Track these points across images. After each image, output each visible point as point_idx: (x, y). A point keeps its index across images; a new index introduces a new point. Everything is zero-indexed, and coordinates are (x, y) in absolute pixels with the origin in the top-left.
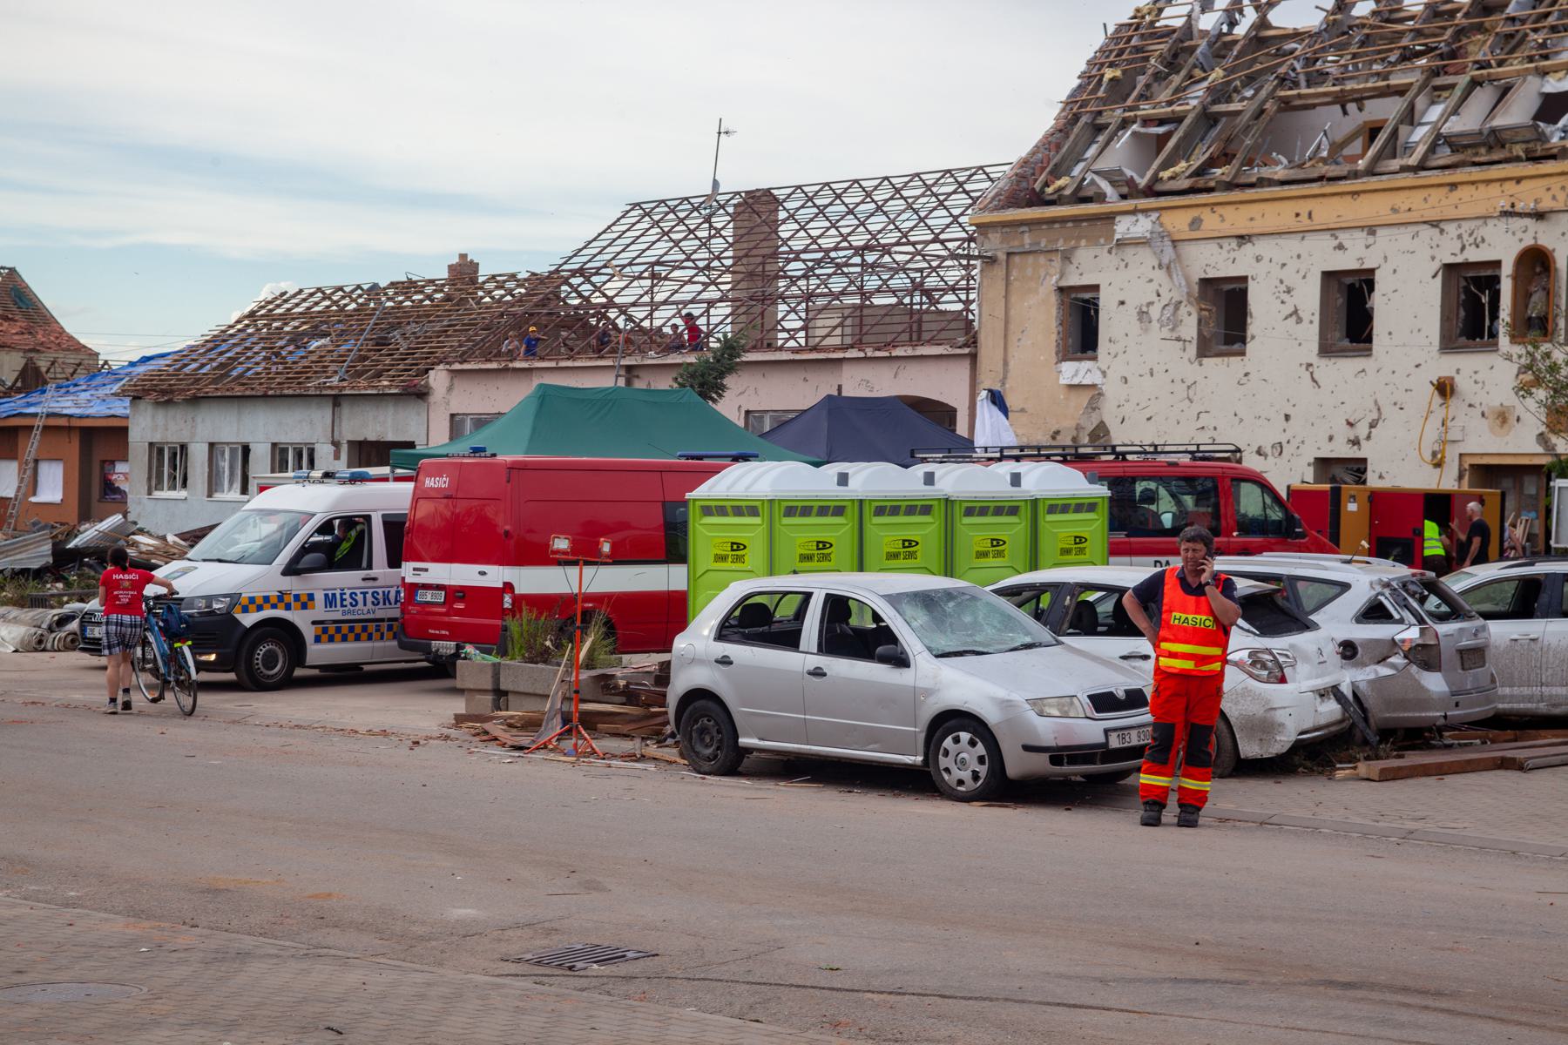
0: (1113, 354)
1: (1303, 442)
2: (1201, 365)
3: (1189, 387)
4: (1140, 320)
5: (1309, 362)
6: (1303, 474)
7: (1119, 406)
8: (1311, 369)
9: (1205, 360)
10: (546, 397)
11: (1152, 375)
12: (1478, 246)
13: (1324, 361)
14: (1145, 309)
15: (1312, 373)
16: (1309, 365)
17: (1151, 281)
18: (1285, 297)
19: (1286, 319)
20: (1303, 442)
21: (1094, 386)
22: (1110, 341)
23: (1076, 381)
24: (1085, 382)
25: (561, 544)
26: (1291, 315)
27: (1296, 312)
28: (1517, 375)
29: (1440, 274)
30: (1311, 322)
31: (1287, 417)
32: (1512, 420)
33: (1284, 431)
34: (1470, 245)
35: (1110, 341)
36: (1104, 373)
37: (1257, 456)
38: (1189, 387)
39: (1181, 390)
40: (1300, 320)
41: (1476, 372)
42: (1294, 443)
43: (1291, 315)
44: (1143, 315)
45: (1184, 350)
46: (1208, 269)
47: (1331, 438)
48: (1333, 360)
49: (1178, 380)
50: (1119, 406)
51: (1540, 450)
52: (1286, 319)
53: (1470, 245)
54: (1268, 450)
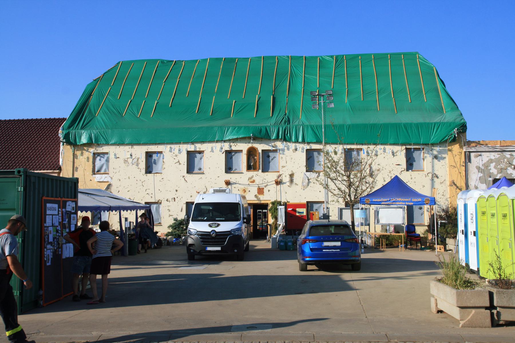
0: (115, 172)
1: (182, 197)
2: (147, 176)
3: (142, 182)
4: (125, 163)
5: (184, 175)
6: (182, 206)
7: (117, 188)
8: (184, 177)
9: (148, 175)
10: (75, 171)
11: (129, 178)
12: (235, 146)
13: (189, 175)
14: (126, 160)
15: (184, 178)
16: (183, 177)
17: (128, 152)
18: (175, 157)
19: (175, 163)
20: (182, 197)
21: (108, 182)
22: (114, 169)
23: (101, 180)
24: (105, 181)
25: (292, 249)
26: (177, 162)
27: (179, 162)
28: (248, 180)
29: (225, 152)
30: (184, 164)
31: (176, 191)
32: (247, 191)
33: (176, 194)
34: (233, 146)
35: (114, 169)
36: (112, 178)
37: (167, 202)
38: (142, 182)
39: (140, 183)
40: (180, 164)
41: (236, 179)
42: (179, 198)
43: (177, 162)
44: (126, 161)
45: (141, 172)
46: (148, 149)
47: (191, 196)
48: (191, 175)
49: (138, 180)
50: (117, 188)
51: (256, 199)
52: (175, 163)
53: (233, 146)
54: (171, 200)
